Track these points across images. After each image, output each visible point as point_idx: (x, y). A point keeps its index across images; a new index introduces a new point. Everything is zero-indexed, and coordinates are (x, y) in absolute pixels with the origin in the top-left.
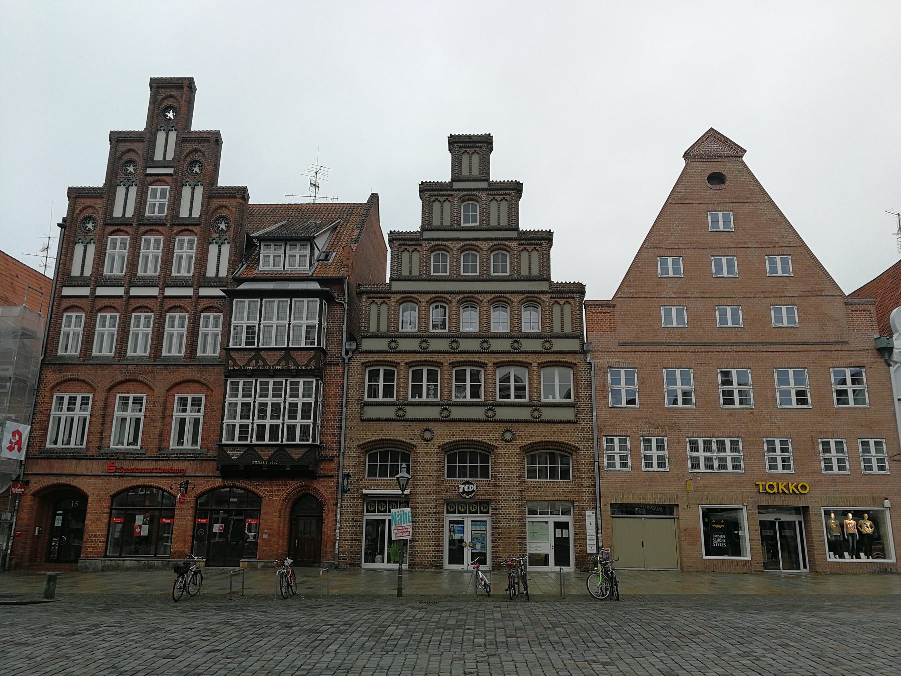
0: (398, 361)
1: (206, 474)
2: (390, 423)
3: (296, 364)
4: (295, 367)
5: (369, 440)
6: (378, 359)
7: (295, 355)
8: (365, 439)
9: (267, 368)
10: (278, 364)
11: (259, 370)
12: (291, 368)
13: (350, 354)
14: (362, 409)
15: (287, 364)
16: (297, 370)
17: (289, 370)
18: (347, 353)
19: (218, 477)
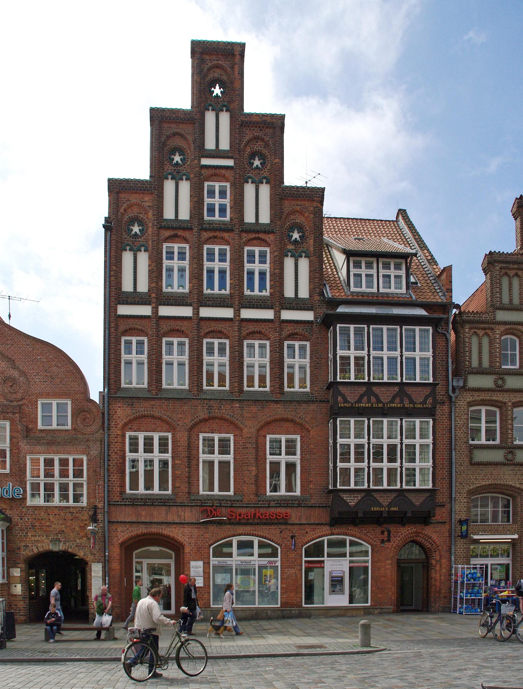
0: (505, 400)
1: (312, 522)
2: (499, 467)
3: (411, 401)
4: (411, 405)
5: (479, 485)
6: (484, 398)
7: (410, 390)
8: (475, 484)
9: (380, 405)
10: (392, 402)
11: (372, 408)
12: (406, 406)
13: (457, 391)
14: (471, 452)
15: (402, 402)
16: (413, 408)
17: (404, 407)
18: (454, 389)
19: (326, 524)
